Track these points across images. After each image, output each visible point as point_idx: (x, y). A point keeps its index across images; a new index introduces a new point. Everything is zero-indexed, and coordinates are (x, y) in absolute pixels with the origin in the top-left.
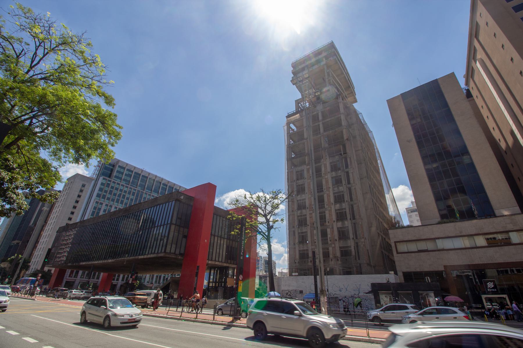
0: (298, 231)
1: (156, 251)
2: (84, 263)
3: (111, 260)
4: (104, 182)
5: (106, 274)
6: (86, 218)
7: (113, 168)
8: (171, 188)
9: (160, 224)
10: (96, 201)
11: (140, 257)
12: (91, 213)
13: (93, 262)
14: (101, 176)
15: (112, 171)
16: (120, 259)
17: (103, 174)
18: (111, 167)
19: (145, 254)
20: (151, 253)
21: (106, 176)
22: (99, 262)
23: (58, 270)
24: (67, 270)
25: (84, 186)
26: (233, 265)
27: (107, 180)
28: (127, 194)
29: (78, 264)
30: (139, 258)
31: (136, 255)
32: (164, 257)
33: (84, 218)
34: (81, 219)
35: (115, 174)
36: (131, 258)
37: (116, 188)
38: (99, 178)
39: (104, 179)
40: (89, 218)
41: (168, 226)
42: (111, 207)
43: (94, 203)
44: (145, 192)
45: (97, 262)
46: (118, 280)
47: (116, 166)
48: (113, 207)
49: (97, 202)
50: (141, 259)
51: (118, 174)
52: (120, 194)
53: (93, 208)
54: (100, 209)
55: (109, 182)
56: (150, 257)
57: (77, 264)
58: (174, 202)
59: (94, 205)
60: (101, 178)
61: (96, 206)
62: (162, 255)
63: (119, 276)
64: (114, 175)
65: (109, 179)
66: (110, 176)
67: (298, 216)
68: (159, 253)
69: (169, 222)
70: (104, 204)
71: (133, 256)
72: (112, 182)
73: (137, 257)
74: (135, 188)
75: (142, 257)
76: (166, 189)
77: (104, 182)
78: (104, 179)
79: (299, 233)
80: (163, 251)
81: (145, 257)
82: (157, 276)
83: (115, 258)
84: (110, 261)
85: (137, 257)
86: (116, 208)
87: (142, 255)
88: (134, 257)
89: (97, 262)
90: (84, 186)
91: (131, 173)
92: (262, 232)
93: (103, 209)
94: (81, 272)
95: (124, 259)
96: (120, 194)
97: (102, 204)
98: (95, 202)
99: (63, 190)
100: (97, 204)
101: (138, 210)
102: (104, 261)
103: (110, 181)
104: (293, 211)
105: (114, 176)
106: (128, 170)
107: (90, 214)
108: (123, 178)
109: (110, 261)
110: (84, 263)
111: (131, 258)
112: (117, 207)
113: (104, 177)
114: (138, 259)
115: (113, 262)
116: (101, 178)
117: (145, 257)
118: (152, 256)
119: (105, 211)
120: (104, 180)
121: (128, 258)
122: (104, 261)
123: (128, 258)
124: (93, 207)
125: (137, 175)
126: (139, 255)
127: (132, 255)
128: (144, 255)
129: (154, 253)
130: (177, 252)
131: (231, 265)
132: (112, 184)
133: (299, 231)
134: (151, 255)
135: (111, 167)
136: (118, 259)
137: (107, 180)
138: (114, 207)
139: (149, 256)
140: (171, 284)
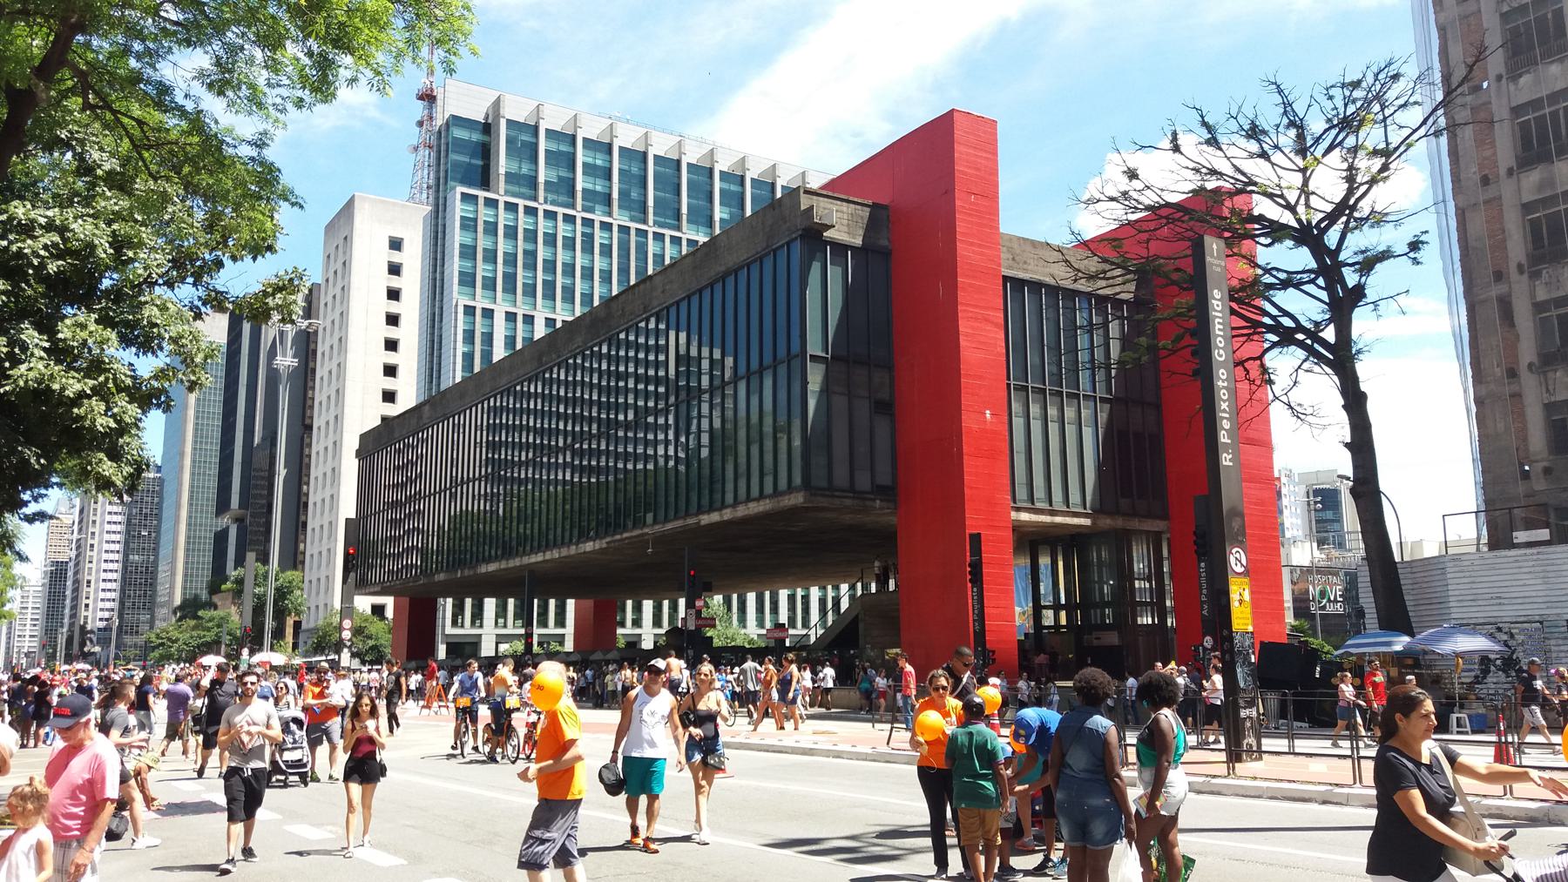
0: (1533, 294)
1: (769, 489)
2: (492, 567)
3: (591, 543)
5: (589, 603)
7: (486, 138)
8: (766, 186)
9: (755, 365)
11: (706, 519)
13: (526, 560)
15: (485, 152)
16: (625, 535)
19: (723, 506)
20: (749, 499)
21: (470, 184)
22: (548, 555)
23: (405, 601)
24: (441, 600)
25: (396, 244)
26: (1150, 522)
29: (472, 573)
30: (703, 523)
31: (687, 514)
32: (807, 508)
33: (439, 385)
35: (503, 163)
36: (669, 526)
45: (539, 558)
46: (637, 623)
47: (498, 124)
51: (514, 168)
56: (746, 513)
57: (466, 572)
62: (798, 499)
63: (638, 609)
64: (502, 171)
66: (485, 181)
67: (1527, 208)
68: (782, 494)
71: (676, 518)
73: (691, 521)
75: (715, 517)
76: (743, 194)
79: (1539, 307)
80: (797, 480)
81: (727, 514)
82: (792, 598)
83: (606, 534)
84: (589, 546)
85: (691, 521)
86: (550, 322)
87: (711, 509)
88: (679, 523)
89: (539, 558)
90: (396, 244)
92: (1300, 328)
94: (490, 604)
95: (642, 535)
99: (327, 280)
101: (645, 312)
102: (564, 552)
104: (1485, 181)
105: (502, 178)
109: (589, 546)
110: (492, 567)
111: (669, 526)
112: (555, 320)
114: (699, 528)
115: (602, 551)
117: (725, 518)
118: (755, 508)
119: (510, 341)
121: (658, 528)
122: (564, 552)
123: (658, 528)
126: (700, 511)
127: (672, 513)
128: (720, 509)
129: (762, 496)
130: (863, 482)
131: (1135, 524)
133: (1542, 295)
134: (751, 505)
136: (618, 537)
139: (741, 511)
140: (861, 626)
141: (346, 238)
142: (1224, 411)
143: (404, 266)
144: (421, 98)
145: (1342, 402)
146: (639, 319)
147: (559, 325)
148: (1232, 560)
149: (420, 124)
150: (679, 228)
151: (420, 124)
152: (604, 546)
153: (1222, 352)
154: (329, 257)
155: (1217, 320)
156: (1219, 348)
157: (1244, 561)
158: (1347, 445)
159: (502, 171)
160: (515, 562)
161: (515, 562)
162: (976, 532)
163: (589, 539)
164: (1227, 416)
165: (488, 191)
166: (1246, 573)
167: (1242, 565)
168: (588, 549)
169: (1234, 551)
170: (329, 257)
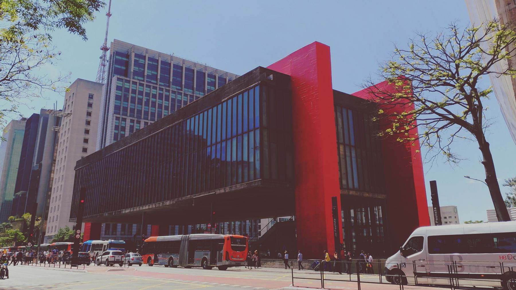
4: (120, 84)
6: (107, 144)
8: (222, 79)
10: (116, 117)
12: (113, 136)
14: (114, 76)
15: (127, 64)
16: (184, 198)
17: (117, 72)
18: (124, 59)
21: (120, 75)
25: (91, 97)
27: (124, 81)
28: (157, 100)
33: (105, 145)
34: (101, 146)
35: (132, 68)
37: (139, 91)
38: (111, 80)
39: (118, 79)
40: (112, 143)
42: (140, 124)
43: (114, 120)
44: (183, 92)
45: (147, 207)
48: (141, 123)
49: (118, 119)
50: (220, 194)
53: (114, 128)
58: (257, 89)
59: (114, 123)
61: (118, 124)
64: (132, 71)
65: (126, 78)
66: (125, 73)
74: (168, 88)
76: (215, 82)
77: (120, 84)
78: (118, 79)
86: (146, 123)
89: (147, 207)
90: (91, 97)
96: (148, 100)
97: (124, 120)
98: (115, 118)
99: (65, 108)
100: (118, 121)
103: (128, 82)
105: (132, 73)
106: (150, 59)
107: (113, 138)
108: (146, 74)
110: (127, 211)
112: (148, 123)
113: (119, 77)
120: (118, 82)
124: (114, 126)
125: (166, 65)
135: (124, 59)
137: (124, 81)
138: (143, 123)
141: (73, 94)
143: (93, 103)
144: (102, 49)
145: (479, 147)
146: (192, 116)
147: (149, 124)
149: (101, 58)
150: (193, 93)
151: (101, 58)
152: (174, 203)
154: (67, 100)
158: (483, 163)
160: (137, 209)
161: (137, 209)
162: (335, 196)
163: (168, 199)
165: (127, 77)
168: (167, 204)
170: (67, 100)
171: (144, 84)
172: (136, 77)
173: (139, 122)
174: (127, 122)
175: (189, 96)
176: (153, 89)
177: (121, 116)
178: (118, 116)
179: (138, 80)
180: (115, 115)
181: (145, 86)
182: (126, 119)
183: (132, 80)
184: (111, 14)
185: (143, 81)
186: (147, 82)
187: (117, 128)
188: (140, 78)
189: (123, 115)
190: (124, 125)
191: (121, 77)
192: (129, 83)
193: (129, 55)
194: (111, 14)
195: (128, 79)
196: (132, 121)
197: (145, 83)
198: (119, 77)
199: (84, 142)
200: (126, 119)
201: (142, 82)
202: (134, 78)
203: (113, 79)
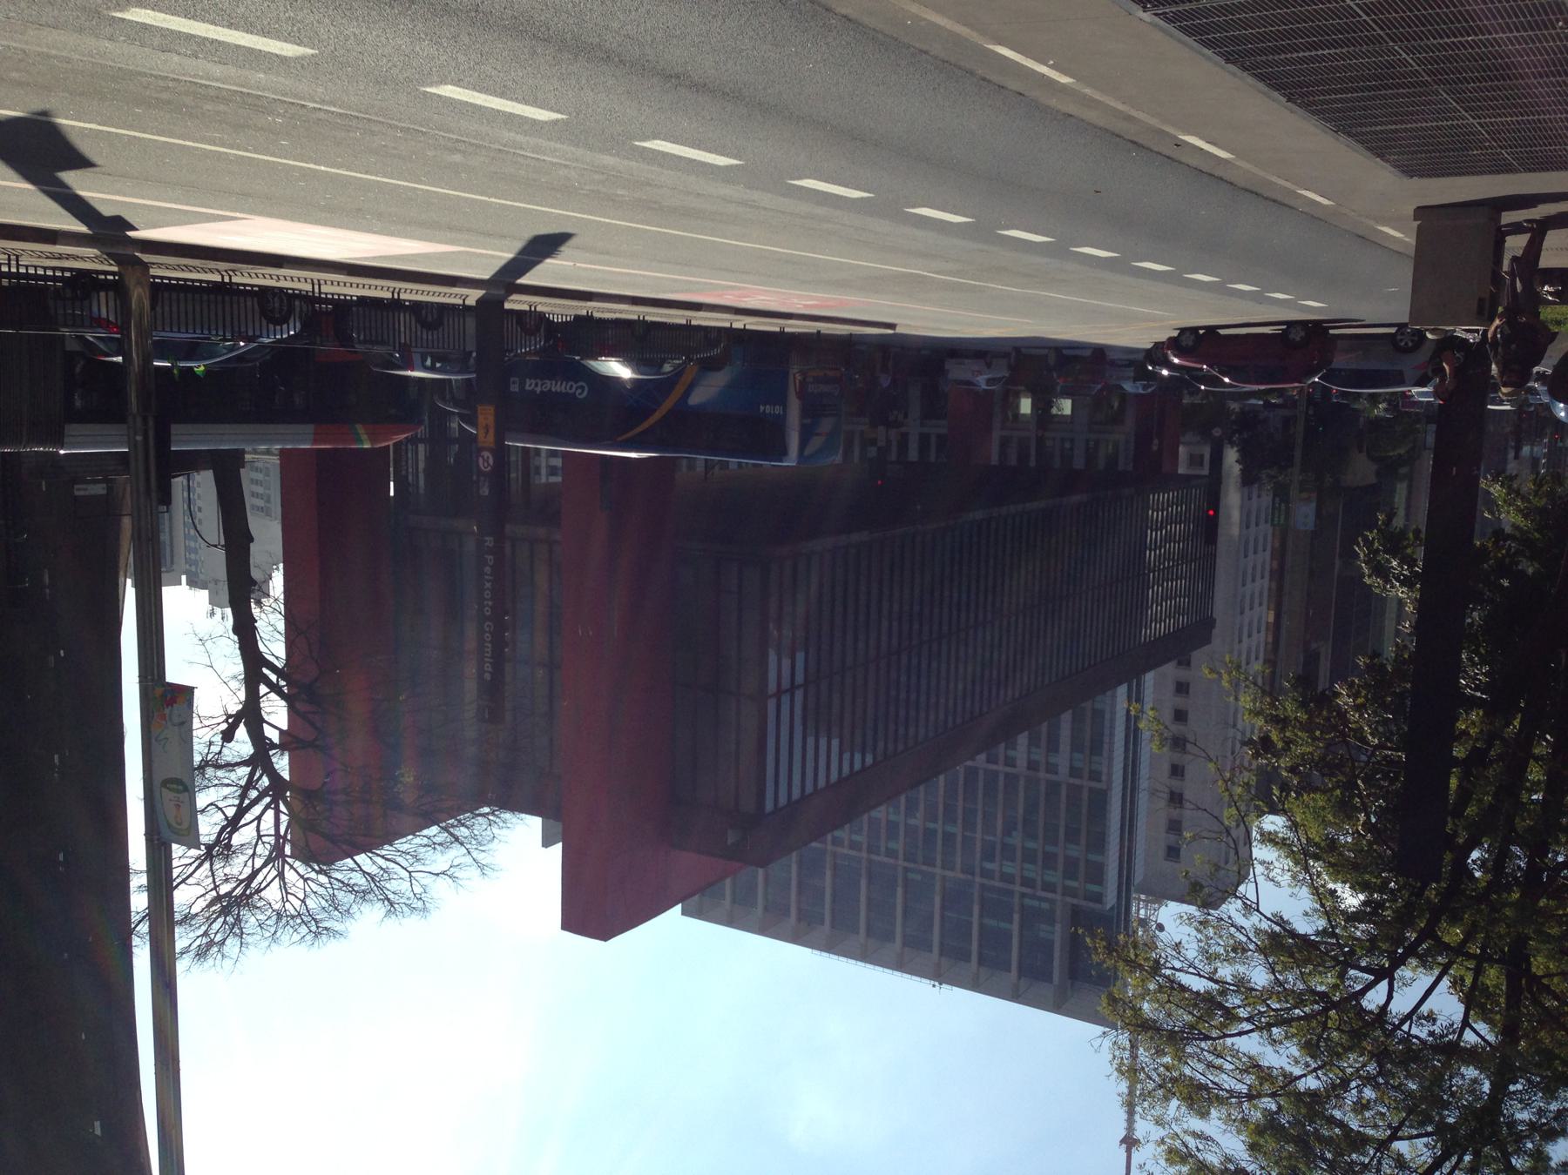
14: (1112, 908)
24: (1130, 468)
25: (1173, 853)
35: (1057, 934)
41: (772, 687)
42: (1029, 762)
43: (1105, 770)
46: (924, 440)
49: (1095, 776)
52: (1008, 832)
54: (1076, 746)
55: (1069, 883)
58: (769, 806)
60: (1111, 899)
61: (1095, 758)
64: (1058, 927)
65: (1075, 901)
66: (1077, 916)
69: (771, 704)
70: (1064, 769)
72: (1059, 890)
78: (1098, 898)
86: (1010, 762)
90: (1173, 853)
91: (986, 921)
93: (1062, 747)
94: (1079, 463)
97: (1074, 772)
98: (1104, 778)
103: (1068, 891)
107: (1107, 716)
113: (1097, 906)
116: (1111, 899)
124: (1105, 754)
132: (1055, 877)
138: (1018, 763)
142: (488, 581)
148: (491, 461)
150: (870, 861)
153: (487, 629)
155: (489, 655)
156: (490, 633)
157: (481, 460)
159: (1058, 927)
164: (486, 577)
165: (1073, 905)
166: (480, 450)
167: (483, 457)
169: (489, 468)
171: (1022, 885)
172: (1045, 906)
173: (1033, 766)
174: (1068, 765)
175: (883, 849)
176: (994, 871)
177: (1086, 783)
178: (1094, 784)
179: (1040, 899)
180: (1102, 786)
181: (1018, 880)
182: (1071, 775)
183: (1058, 897)
184: (1124, 1146)
185: (1023, 895)
186: (1011, 893)
187: (1097, 745)
188: (1036, 903)
189: (1080, 787)
190: (1076, 755)
191: (1091, 905)
192: (1064, 887)
193: (1070, 978)
194: (1124, 1146)
195: (1069, 900)
196: (1051, 768)
197: (1018, 888)
198: (1097, 906)
199: (1187, 712)
200: (1071, 775)
201: (1028, 891)
202: (1052, 902)
203: (1115, 900)
